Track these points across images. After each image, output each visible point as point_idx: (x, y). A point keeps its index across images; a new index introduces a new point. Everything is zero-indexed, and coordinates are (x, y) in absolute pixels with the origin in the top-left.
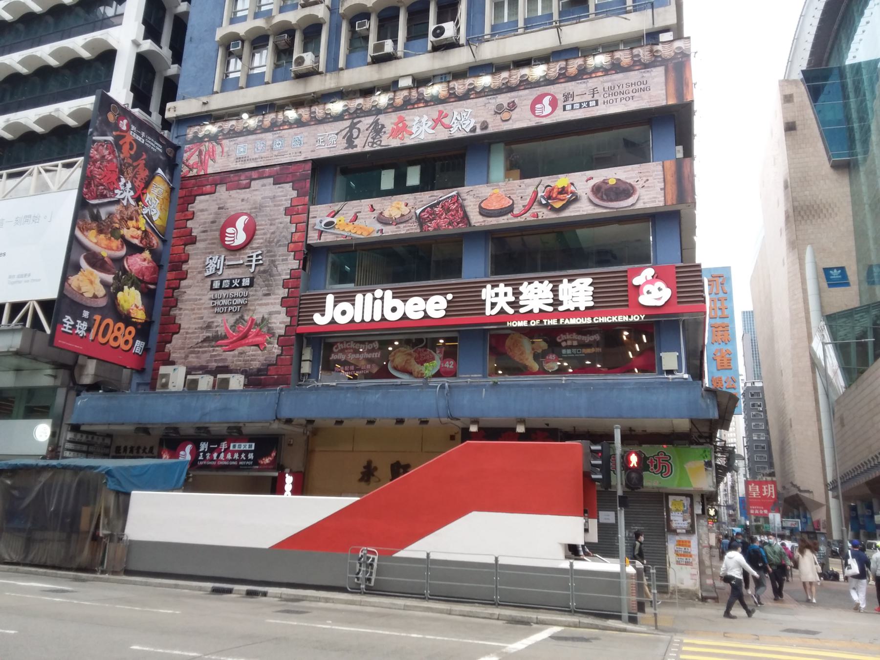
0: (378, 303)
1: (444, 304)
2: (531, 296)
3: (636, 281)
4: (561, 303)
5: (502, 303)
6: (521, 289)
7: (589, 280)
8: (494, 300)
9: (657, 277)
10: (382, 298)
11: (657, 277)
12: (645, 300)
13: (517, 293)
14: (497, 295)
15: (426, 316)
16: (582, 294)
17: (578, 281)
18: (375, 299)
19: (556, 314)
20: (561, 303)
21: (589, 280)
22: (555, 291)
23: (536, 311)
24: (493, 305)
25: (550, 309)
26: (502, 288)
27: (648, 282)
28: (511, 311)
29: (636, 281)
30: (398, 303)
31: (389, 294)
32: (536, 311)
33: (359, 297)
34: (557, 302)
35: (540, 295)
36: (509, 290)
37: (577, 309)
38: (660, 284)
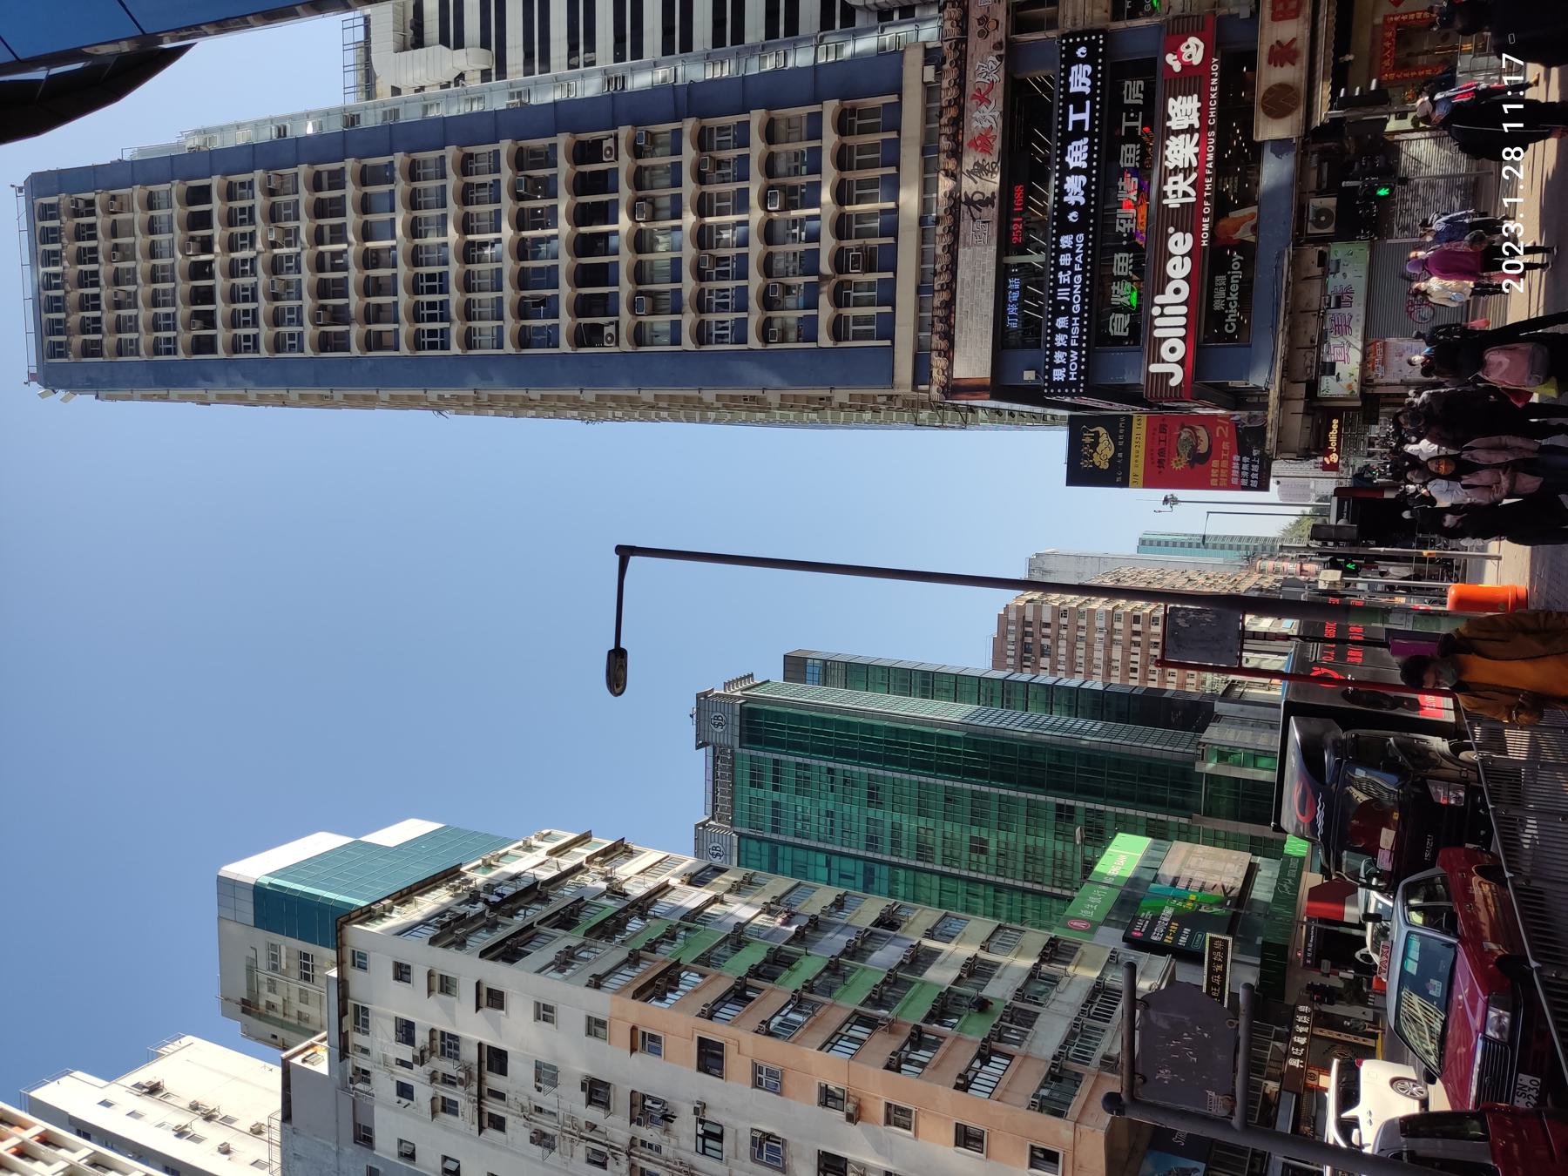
0: (1167, 311)
1: (1179, 236)
2: (1180, 157)
3: (1177, 67)
4: (1191, 126)
5: (1184, 186)
6: (1171, 167)
7: (1171, 101)
8: (1180, 194)
9: (1175, 50)
10: (1162, 306)
11: (1175, 50)
12: (1197, 59)
13: (1176, 170)
14: (1175, 192)
15: (1189, 254)
16: (1183, 107)
17: (1171, 112)
18: (1162, 315)
19: (1204, 128)
20: (1191, 126)
21: (1171, 101)
22: (1177, 133)
23: (1197, 150)
24: (1185, 194)
25: (1196, 136)
26: (1169, 188)
27: (1179, 59)
28: (1194, 176)
29: (1177, 67)
30: (1170, 287)
31: (1158, 299)
32: (1197, 150)
33: (1157, 333)
34: (1190, 130)
35: (1181, 147)
36: (1171, 180)
37: (1199, 110)
38: (1183, 48)
